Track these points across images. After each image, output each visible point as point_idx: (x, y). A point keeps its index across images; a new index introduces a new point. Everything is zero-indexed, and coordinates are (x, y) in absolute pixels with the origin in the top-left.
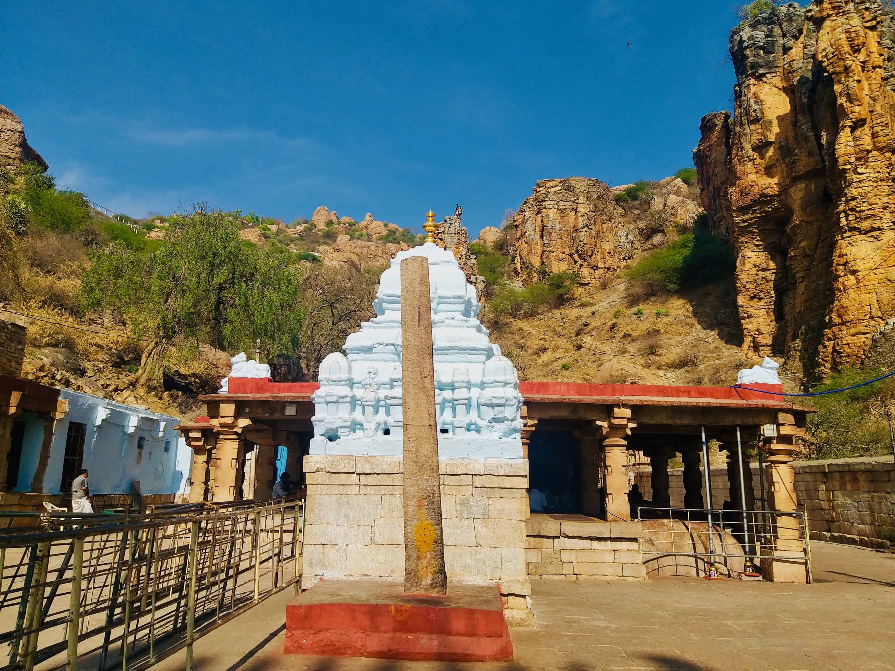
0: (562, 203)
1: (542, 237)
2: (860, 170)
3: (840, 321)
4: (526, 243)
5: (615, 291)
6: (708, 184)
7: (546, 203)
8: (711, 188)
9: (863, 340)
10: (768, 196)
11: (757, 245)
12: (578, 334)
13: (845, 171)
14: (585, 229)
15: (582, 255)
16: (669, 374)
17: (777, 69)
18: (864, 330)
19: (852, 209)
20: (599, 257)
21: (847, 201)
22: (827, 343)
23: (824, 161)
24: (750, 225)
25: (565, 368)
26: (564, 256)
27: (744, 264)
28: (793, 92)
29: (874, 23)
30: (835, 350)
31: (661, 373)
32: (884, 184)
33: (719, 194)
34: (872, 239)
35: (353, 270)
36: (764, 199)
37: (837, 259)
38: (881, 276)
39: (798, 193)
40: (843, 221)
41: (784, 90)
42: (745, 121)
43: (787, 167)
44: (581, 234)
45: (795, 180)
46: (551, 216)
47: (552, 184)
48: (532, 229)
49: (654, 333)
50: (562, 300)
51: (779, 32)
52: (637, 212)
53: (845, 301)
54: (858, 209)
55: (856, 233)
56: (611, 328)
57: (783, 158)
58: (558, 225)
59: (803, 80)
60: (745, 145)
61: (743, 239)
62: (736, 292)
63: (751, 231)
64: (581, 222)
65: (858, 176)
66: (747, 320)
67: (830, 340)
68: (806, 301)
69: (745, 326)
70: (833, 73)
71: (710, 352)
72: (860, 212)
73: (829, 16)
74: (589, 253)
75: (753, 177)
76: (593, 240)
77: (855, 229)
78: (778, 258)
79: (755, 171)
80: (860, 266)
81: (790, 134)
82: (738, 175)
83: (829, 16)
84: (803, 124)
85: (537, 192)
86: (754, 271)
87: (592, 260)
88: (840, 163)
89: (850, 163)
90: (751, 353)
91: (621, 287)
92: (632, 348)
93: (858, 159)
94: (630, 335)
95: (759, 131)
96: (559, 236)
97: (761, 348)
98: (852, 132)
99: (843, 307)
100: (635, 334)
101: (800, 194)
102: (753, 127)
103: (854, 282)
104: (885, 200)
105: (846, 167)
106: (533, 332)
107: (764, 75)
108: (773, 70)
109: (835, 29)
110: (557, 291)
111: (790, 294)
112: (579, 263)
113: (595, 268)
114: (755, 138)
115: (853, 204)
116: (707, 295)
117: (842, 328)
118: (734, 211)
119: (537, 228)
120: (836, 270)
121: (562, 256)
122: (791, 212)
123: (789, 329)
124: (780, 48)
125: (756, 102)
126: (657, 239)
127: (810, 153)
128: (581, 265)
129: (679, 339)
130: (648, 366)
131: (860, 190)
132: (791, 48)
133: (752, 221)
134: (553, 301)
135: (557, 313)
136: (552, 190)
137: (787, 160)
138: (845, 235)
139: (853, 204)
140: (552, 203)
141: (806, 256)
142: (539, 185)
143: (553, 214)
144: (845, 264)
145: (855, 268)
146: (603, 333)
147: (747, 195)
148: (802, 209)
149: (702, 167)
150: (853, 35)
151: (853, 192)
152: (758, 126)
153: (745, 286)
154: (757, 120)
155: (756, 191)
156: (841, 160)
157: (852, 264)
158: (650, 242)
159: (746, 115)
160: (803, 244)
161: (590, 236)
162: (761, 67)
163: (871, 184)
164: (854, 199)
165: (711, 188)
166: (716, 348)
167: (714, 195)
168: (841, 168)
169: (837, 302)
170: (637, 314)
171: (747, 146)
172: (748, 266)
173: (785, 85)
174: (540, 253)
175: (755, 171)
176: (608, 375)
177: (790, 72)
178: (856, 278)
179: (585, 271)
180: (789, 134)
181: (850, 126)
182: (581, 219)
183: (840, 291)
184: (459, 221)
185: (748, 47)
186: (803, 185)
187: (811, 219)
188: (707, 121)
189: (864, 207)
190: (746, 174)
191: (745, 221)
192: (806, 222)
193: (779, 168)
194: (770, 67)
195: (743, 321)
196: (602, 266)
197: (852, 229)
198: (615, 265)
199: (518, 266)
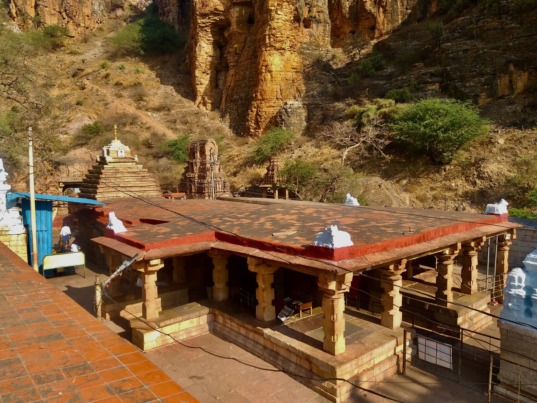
2: (279, 12)
5: (95, 46)
9: (272, 110)
10: (218, 11)
11: (208, 40)
12: (74, 76)
13: (271, 10)
16: (155, 115)
18: (273, 105)
19: (273, 35)
20: (80, 18)
21: (270, 29)
22: (254, 109)
24: (208, 26)
25: (78, 104)
30: (257, 114)
31: (150, 114)
32: (288, 23)
34: (280, 54)
36: (216, 12)
38: (283, 76)
39: (235, 12)
49: (137, 85)
50: (56, 47)
62: (195, 68)
63: (206, 30)
66: (200, 86)
67: (255, 107)
68: (237, 81)
69: (198, 89)
71: (177, 103)
72: (277, 37)
77: (273, 46)
78: (218, 51)
80: (274, 68)
86: (206, 55)
88: (270, 5)
90: (201, 106)
91: (99, 43)
92: (125, 93)
93: (278, 5)
94: (121, 84)
97: (208, 104)
99: (264, 91)
100: (125, 83)
103: (270, 77)
104: (288, 33)
110: (52, 39)
111: (223, 73)
112: (67, 20)
113: (78, 25)
115: (274, 31)
116: (165, 62)
117: (263, 102)
118: (198, 15)
121: (53, 12)
122: (229, 24)
123: (224, 95)
126: (119, 12)
128: (68, 22)
129: (155, 91)
130: (139, 108)
131: (278, 24)
134: (50, 47)
135: (53, 56)
138: (267, 49)
139: (274, 31)
141: (237, 54)
144: (266, 66)
146: (99, 78)
147: (206, 6)
148: (238, 25)
151: (274, 24)
153: (200, 65)
155: (212, 5)
160: (235, 46)
163: (283, 22)
164: (274, 29)
166: (180, 100)
169: (260, 87)
170: (121, 69)
172: (203, 53)
176: (114, 112)
178: (271, 75)
187: (241, 31)
189: (279, 35)
191: (204, 23)
192: (239, 33)
195: (197, 86)
196: (83, 25)
197: (271, 46)
198: (92, 26)
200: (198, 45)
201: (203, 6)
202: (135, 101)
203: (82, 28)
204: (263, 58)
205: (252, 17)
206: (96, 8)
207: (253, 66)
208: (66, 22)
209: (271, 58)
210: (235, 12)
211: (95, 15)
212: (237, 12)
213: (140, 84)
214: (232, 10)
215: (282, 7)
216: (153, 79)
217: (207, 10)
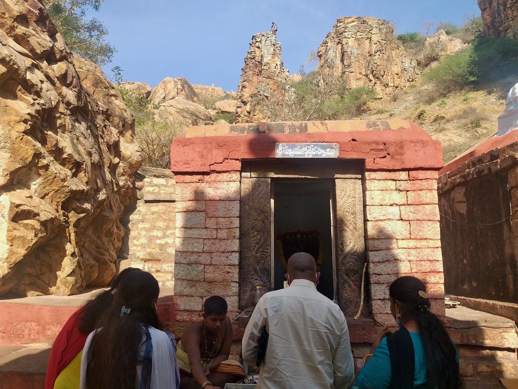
0: (359, 34)
1: (342, 61)
5: (406, 101)
7: (346, 34)
14: (379, 53)
15: (375, 75)
20: (389, 78)
26: (361, 76)
35: (186, 86)
44: (374, 58)
46: (350, 44)
47: (350, 20)
58: (355, 51)
64: (374, 48)
74: (382, 73)
76: (385, 62)
85: (337, 27)
87: (384, 79)
91: (411, 98)
92: (448, 126)
94: (444, 118)
96: (357, 59)
112: (373, 82)
113: (386, 86)
121: (359, 76)
126: (434, 65)
128: (375, 83)
134: (354, 110)
136: (350, 25)
140: (351, 33)
142: (339, 21)
143: (351, 42)
158: (429, 67)
161: (382, 59)
179: (379, 88)
182: (374, 46)
184: (274, 36)
196: (392, 85)
198: (402, 84)
202: (466, 131)
206: (407, 65)
208: (372, 85)
211: (406, 72)
213: (473, 110)
216: (493, 103)
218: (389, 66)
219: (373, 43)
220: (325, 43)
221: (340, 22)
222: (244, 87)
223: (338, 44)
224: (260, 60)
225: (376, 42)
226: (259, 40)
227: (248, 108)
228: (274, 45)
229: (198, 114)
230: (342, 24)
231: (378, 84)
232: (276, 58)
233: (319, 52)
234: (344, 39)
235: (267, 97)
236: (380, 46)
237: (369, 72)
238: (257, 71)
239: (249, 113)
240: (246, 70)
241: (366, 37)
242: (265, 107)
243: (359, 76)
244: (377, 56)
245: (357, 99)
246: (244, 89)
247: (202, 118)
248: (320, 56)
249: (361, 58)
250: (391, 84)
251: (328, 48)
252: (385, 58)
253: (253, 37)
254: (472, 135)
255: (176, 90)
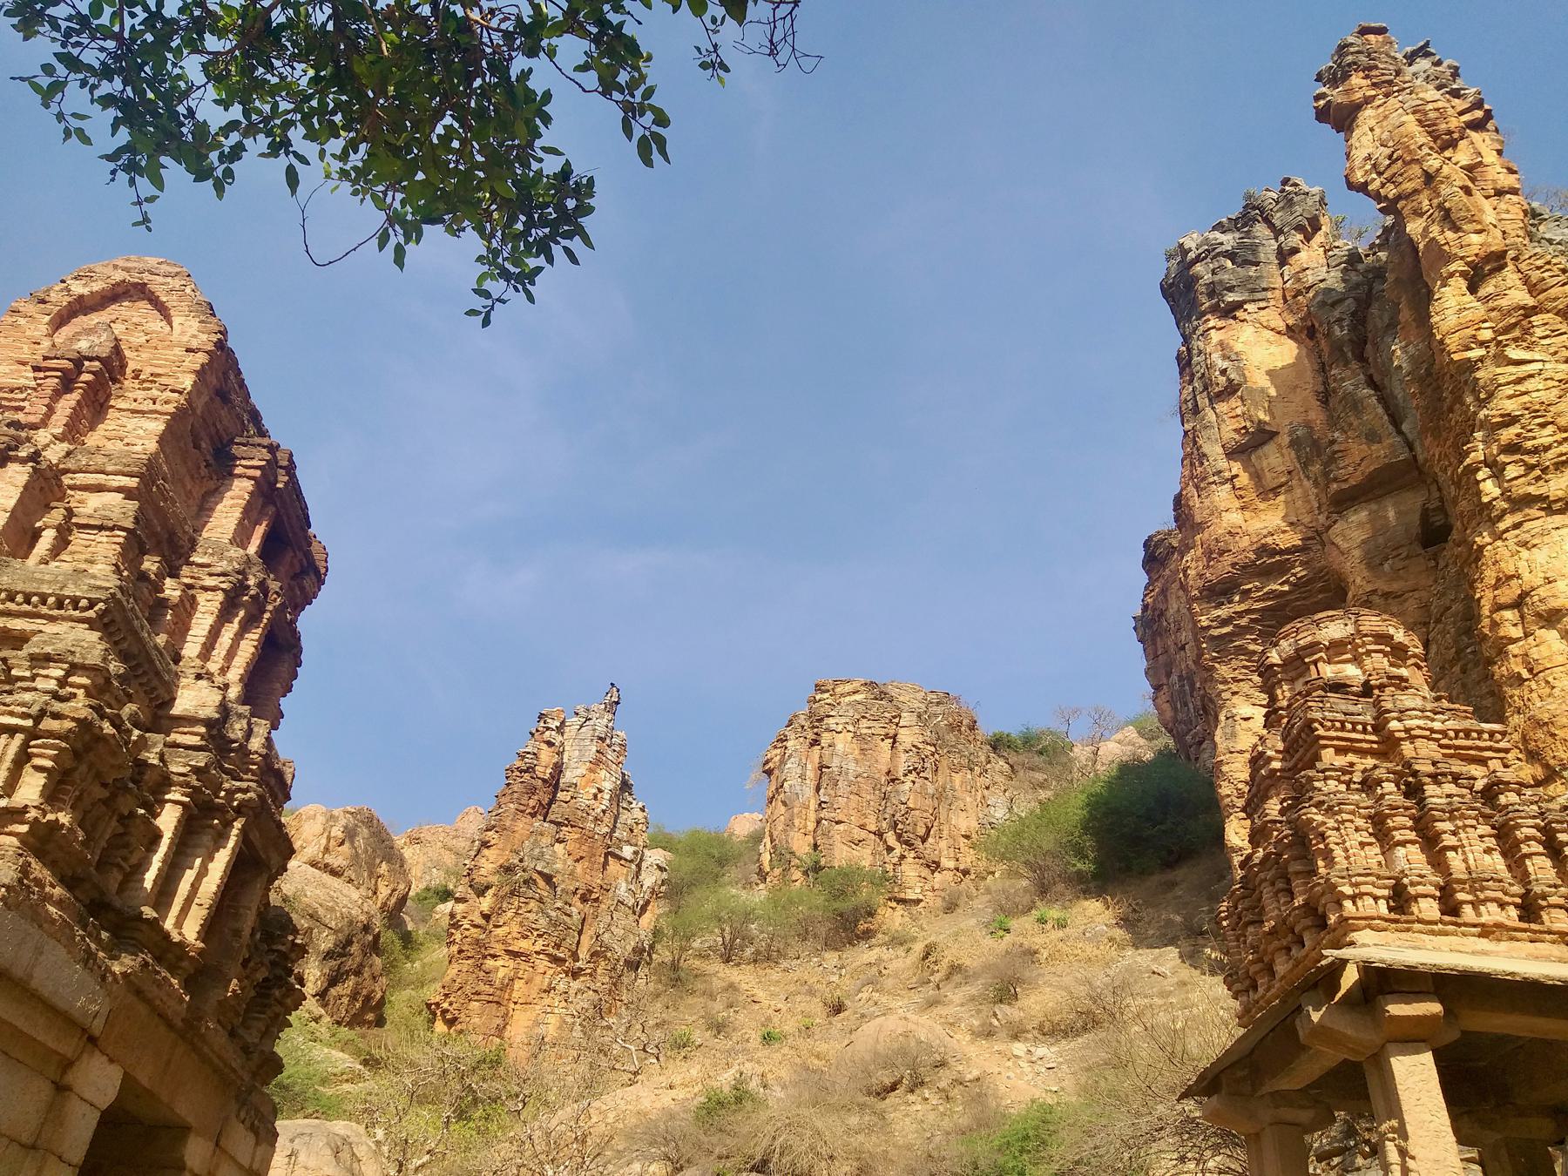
0: (864, 723)
1: (818, 789)
2: (1514, 353)
3: (1539, 772)
4: (784, 803)
6: (1169, 675)
8: (1174, 678)
13: (1471, 366)
14: (912, 777)
15: (907, 835)
16: (1041, 1051)
17: (1269, 294)
19: (1512, 448)
20: (943, 844)
23: (1411, 447)
26: (864, 834)
27: (1234, 735)
28: (1311, 332)
29: (1479, 114)
31: (1019, 1048)
33: (1192, 685)
36: (1267, 561)
37: (1489, 594)
40: (1490, 489)
41: (1290, 331)
42: (1203, 401)
43: (1316, 484)
45: (1342, 502)
46: (840, 747)
47: (848, 688)
48: (797, 773)
51: (1268, 232)
52: (1040, 776)
53: (1541, 708)
54: (1529, 444)
55: (1534, 512)
56: (925, 958)
57: (1305, 466)
58: (852, 766)
59: (1329, 300)
60: (1206, 449)
61: (1223, 670)
63: (1242, 650)
65: (1511, 369)
70: (1399, 198)
72: (1535, 451)
73: (1368, 100)
74: (921, 831)
75: (1234, 518)
76: (929, 802)
77: (1529, 500)
79: (1237, 504)
81: (1317, 416)
82: (1198, 519)
83: (1368, 100)
84: (1343, 380)
85: (815, 702)
88: (1453, 348)
89: (1482, 344)
92: (956, 994)
95: (1239, 411)
98: (1473, 289)
99: (1540, 724)
101: (1358, 536)
102: (1222, 407)
105: (1470, 354)
106: (761, 995)
107: (1239, 305)
108: (1259, 296)
109: (1386, 117)
112: (898, 852)
113: (935, 866)
114: (1229, 431)
115: (1508, 434)
116: (1172, 885)
119: (810, 774)
120: (1495, 625)
121: (858, 834)
124: (1273, 258)
125: (1225, 357)
127: (1372, 437)
128: (903, 857)
130: (988, 1033)
132: (1295, 251)
133: (1244, 622)
135: (831, 958)
136: (848, 699)
137: (1316, 468)
138: (1502, 526)
139: (1508, 434)
142: (819, 688)
143: (843, 743)
144: (1518, 604)
145: (1554, 604)
147: (1222, 553)
148: (1370, 566)
149: (1155, 644)
150: (1432, 115)
152: (1234, 402)
154: (1231, 389)
156: (1452, 342)
157: (1542, 592)
159: (1206, 388)
161: (923, 793)
162: (1231, 289)
164: (1509, 420)
165: (1174, 678)
167: (1182, 691)
168: (1456, 357)
171: (1214, 451)
173: (1290, 322)
174: (811, 826)
175: (1237, 504)
177: (1299, 293)
179: (911, 871)
180: (1312, 415)
181: (1463, 274)
183: (1520, 681)
185: (1198, 259)
186: (1363, 515)
187: (1396, 587)
188: (1157, 546)
189: (1545, 436)
190: (1216, 512)
193: (1298, 492)
194: (1253, 291)
196: (951, 864)
199: (766, 858)
200: (1222, 717)
201: (1210, 559)
203: (948, 876)
204: (1490, 575)
205: (1438, 520)
207: (1474, 675)
209: (1539, 556)
210: (1352, 531)
212: (1360, 525)
214: (1338, 527)
215: (1527, 331)
217: (1224, 566)
218: (943, 811)
219: (901, 748)
220: (782, 741)
221: (823, 692)
222: (485, 844)
223: (812, 745)
224: (547, 777)
225: (909, 747)
226: (555, 724)
227: (486, 903)
228: (602, 739)
229: (321, 912)
230: (826, 695)
231: (910, 860)
232: (603, 773)
233: (767, 762)
234: (825, 735)
235: (548, 879)
236: (916, 759)
237: (884, 825)
238: (532, 803)
239: (486, 917)
240: (503, 800)
241: (883, 732)
242: (533, 905)
243: (858, 834)
244: (908, 785)
245: (841, 894)
246: (485, 852)
247: (333, 924)
248: (769, 773)
249: (866, 787)
250: (945, 863)
251: (788, 752)
252: (931, 790)
253: (541, 716)
254: (982, 1025)
255: (324, 841)
